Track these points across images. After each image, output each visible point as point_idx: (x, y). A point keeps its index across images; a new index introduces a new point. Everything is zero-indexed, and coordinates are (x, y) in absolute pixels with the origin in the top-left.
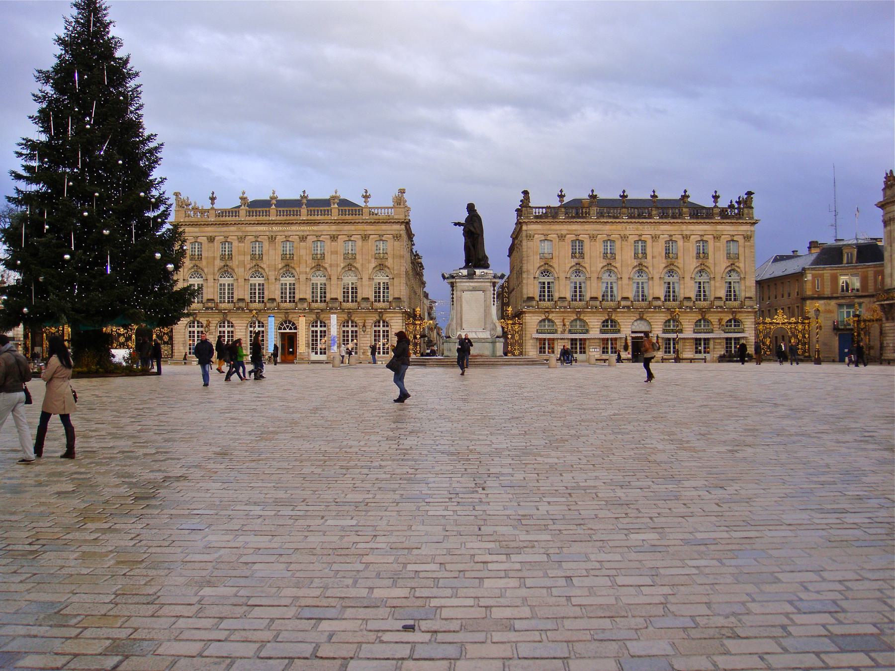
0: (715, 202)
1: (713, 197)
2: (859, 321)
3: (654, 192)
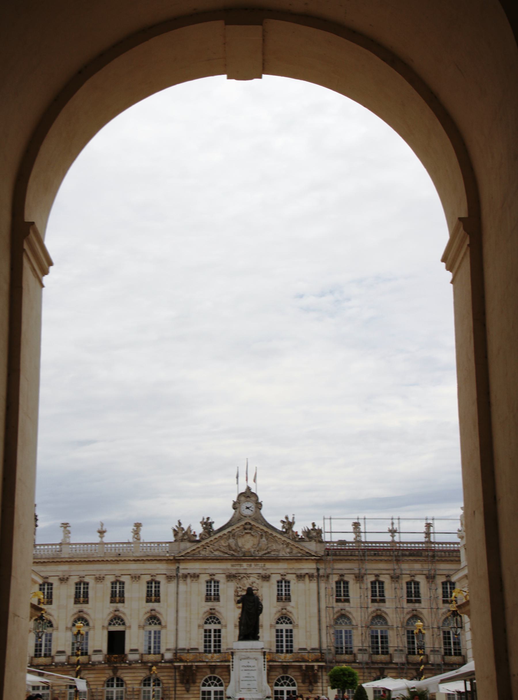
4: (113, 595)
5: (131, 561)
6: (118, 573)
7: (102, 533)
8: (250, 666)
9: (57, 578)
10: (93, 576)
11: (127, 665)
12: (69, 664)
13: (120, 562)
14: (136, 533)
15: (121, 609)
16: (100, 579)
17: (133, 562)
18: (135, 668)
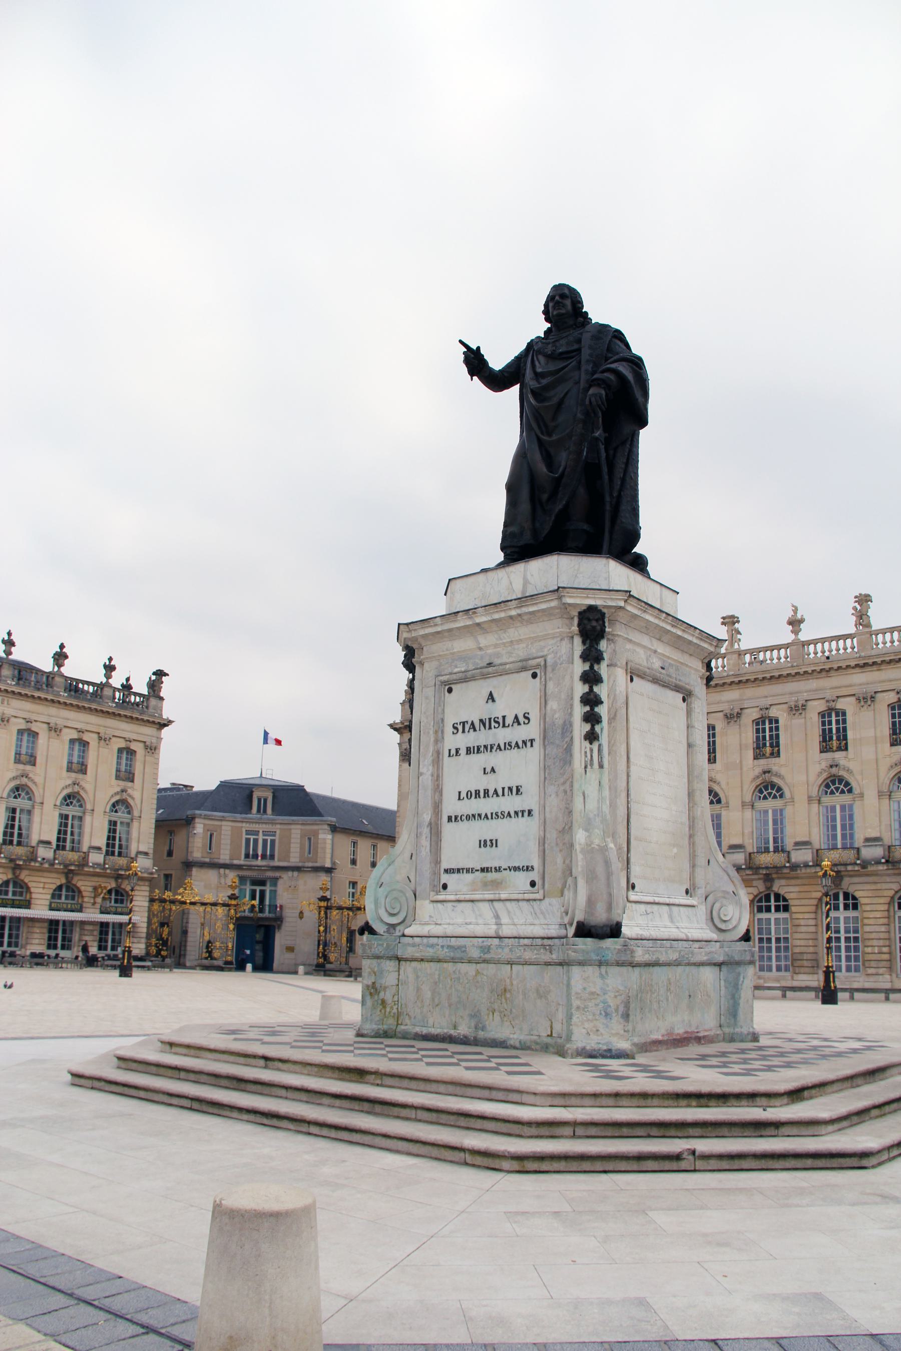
0: (108, 676)
1: (105, 666)
2: (327, 908)
3: (9, 634)
4: (826, 737)
5: (853, 668)
6: (829, 695)
7: (795, 623)
8: (502, 723)
9: (721, 714)
10: (785, 706)
11: (856, 868)
12: (750, 868)
13: (832, 673)
14: (862, 617)
15: (842, 762)
16: (798, 709)
17: (857, 670)
18: (875, 874)
